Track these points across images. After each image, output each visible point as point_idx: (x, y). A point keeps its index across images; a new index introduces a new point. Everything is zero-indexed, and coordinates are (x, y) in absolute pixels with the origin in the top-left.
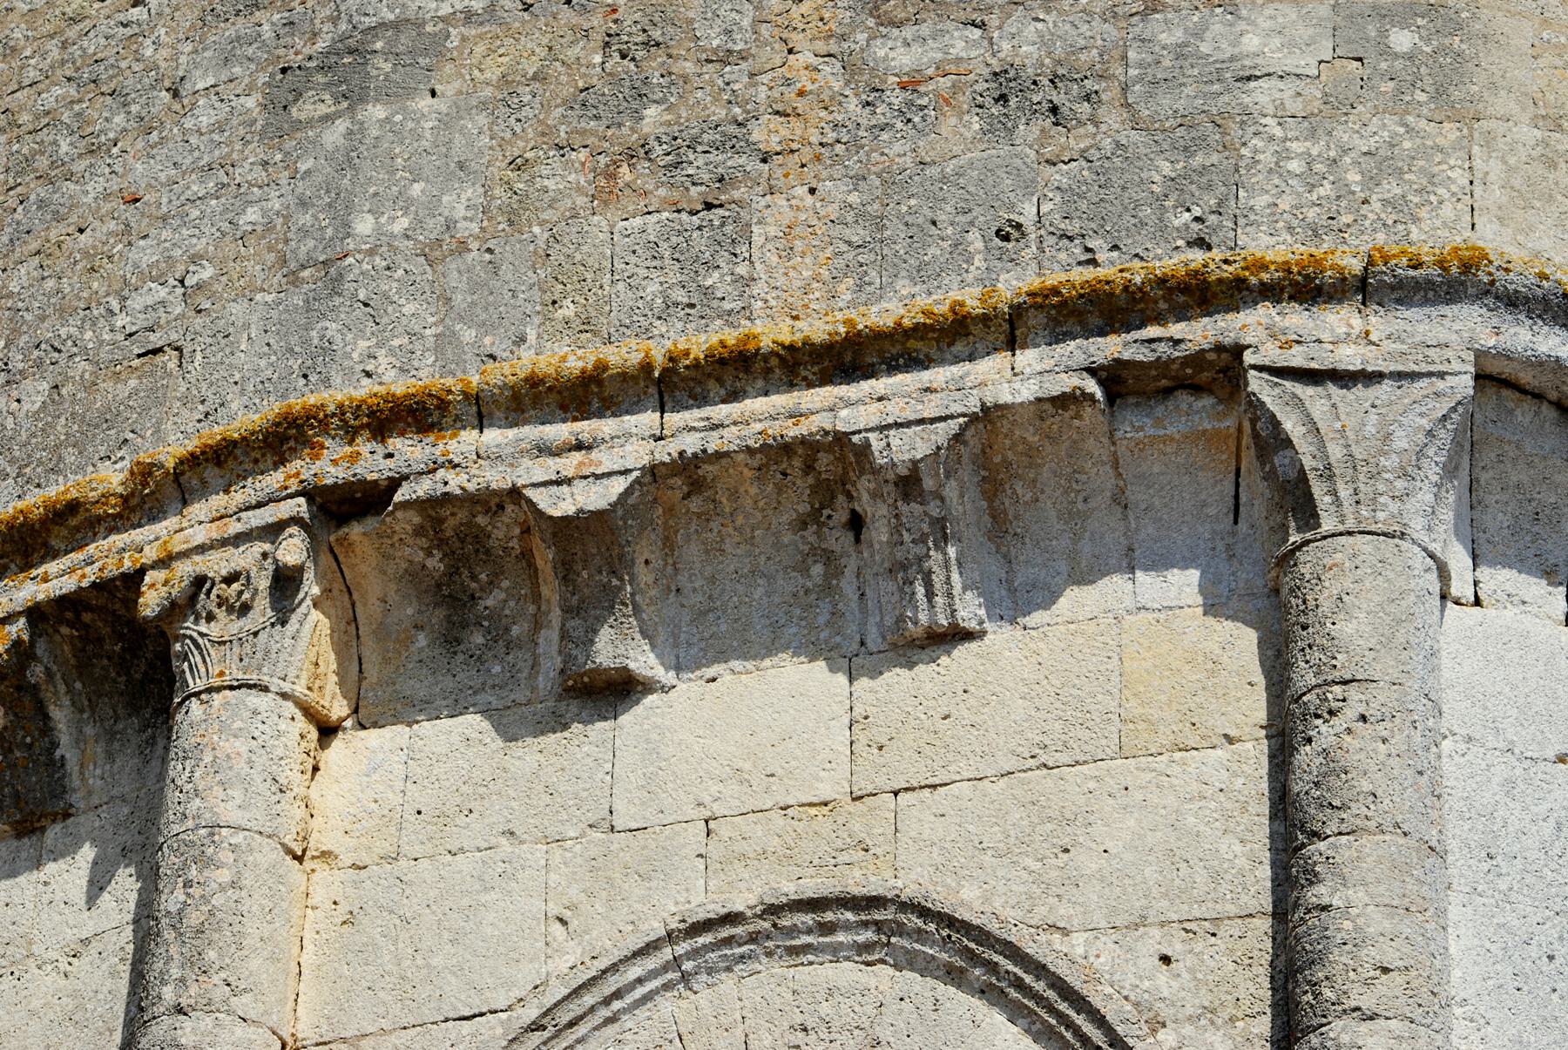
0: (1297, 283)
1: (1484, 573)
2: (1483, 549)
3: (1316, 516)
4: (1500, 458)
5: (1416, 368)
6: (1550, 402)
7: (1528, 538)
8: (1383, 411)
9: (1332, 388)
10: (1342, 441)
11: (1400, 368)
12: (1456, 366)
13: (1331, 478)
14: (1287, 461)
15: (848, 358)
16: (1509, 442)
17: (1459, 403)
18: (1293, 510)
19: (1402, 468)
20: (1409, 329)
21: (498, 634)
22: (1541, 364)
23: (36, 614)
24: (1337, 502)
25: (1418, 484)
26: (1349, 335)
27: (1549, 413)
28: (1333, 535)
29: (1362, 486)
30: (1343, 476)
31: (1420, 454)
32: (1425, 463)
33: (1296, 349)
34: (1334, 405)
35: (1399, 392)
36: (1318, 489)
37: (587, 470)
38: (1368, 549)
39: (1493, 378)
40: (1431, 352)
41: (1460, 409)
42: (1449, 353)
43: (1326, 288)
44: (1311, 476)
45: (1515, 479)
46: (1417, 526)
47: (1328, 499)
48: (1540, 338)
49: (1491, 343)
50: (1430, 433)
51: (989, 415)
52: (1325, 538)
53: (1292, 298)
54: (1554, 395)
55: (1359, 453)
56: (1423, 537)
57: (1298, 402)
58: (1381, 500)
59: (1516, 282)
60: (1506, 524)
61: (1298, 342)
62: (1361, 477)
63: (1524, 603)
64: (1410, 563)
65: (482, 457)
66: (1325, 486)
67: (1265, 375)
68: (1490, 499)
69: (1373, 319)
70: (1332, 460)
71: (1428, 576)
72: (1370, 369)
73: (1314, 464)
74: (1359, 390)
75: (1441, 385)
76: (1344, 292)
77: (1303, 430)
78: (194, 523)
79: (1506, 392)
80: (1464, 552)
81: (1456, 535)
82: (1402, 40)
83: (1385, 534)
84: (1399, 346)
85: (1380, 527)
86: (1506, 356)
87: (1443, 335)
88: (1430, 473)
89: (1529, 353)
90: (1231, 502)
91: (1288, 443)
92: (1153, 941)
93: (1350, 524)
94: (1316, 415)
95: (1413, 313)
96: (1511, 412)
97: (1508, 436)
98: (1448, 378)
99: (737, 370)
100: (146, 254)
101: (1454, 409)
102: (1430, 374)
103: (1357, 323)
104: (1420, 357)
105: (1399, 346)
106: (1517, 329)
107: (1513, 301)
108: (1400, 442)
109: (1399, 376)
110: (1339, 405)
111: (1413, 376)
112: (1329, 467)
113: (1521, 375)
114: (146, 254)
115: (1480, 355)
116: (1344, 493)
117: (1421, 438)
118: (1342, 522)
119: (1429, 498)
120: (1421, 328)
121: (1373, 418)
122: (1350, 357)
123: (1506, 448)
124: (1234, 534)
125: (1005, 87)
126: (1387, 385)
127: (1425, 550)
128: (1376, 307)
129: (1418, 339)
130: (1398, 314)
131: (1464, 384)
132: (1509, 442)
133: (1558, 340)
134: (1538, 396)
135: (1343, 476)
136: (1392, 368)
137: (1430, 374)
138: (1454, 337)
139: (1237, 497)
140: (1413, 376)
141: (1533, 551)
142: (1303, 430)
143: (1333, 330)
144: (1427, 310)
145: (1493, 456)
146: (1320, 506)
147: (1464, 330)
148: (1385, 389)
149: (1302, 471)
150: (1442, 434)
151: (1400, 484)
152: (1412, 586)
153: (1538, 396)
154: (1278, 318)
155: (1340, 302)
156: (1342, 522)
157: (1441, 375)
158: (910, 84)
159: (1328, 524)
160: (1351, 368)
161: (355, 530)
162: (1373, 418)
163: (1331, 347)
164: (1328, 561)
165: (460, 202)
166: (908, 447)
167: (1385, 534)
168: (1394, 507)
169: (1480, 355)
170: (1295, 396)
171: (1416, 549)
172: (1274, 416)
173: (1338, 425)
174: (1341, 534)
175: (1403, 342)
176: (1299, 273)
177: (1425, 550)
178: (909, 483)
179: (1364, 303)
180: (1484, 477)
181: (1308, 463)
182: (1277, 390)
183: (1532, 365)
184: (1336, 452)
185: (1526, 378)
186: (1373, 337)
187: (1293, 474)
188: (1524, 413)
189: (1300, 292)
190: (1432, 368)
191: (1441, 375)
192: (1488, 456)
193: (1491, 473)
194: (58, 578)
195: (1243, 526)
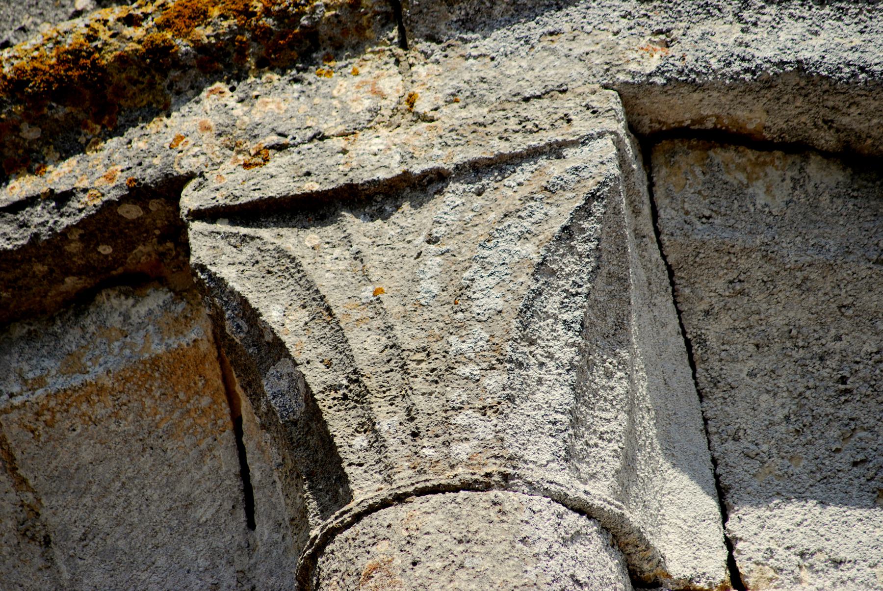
0: (267, 31)
1: (746, 521)
2: (739, 471)
3: (343, 479)
4: (738, 287)
5: (505, 148)
6: (827, 155)
7: (834, 432)
8: (451, 245)
9: (353, 224)
10: (378, 322)
11: (475, 153)
12: (582, 126)
13: (361, 398)
14: (284, 384)
16: (747, 251)
17: (593, 197)
18: (310, 476)
19: (496, 348)
20: (490, 74)
22: (768, 84)
24: (378, 443)
25: (534, 372)
26: (375, 111)
27: (823, 176)
28: (372, 509)
29: (420, 402)
30: (384, 389)
31: (527, 312)
32: (542, 328)
33: (279, 160)
34: (357, 256)
35: (478, 202)
36: (340, 424)
38: (435, 521)
40: (533, 110)
41: (598, 209)
42: (568, 104)
43: (323, 30)
44: (325, 402)
45: (779, 321)
46: (540, 457)
47: (360, 441)
48: (761, 32)
49: (652, 63)
50: (541, 268)
52: (357, 518)
53: (264, 64)
54: (827, 139)
55: (406, 336)
56: (562, 479)
57: (289, 266)
58: (460, 419)
60: (780, 414)
61: (280, 148)
62: (419, 384)
63: (837, 563)
64: (527, 530)
66: (354, 417)
67: (222, 227)
68: (737, 372)
69: (421, 71)
70: (361, 361)
71: (579, 549)
72: (417, 169)
73: (329, 378)
74: (406, 217)
75: (554, 169)
76: (360, 29)
77: (303, 315)
79: (719, 156)
80: (694, 487)
81: (670, 453)
83: (468, 486)
84: (475, 112)
85: (463, 473)
86: (686, 82)
87: (554, 70)
88: (555, 347)
89: (736, 67)
90: (234, 485)
91: (278, 349)
93: (404, 479)
94: (324, 280)
95: (495, 41)
96: (739, 192)
97: (740, 239)
98: (568, 152)
101: (584, 211)
102: (533, 154)
103: (392, 84)
104: (512, 124)
105: (475, 112)
106: (708, 25)
108: (489, 297)
109: (475, 170)
110: (366, 251)
111: (501, 165)
112: (356, 377)
113: (741, 114)
115: (632, 96)
116: (388, 420)
117: (525, 280)
118: (388, 480)
119: (562, 395)
120: (512, 67)
121: (433, 262)
122: (378, 156)
123: (743, 264)
124: (249, 548)
126: (455, 194)
127: (561, 499)
128: (424, 45)
129: (511, 86)
130: (469, 49)
131: (601, 156)
132: (747, 251)
133: (799, 28)
134: (797, 148)
135: (384, 389)
136: (458, 159)
137: (533, 154)
138: (579, 67)
139: (244, 473)
140: (501, 165)
141: (847, 456)
142: (303, 315)
143: (345, 109)
144: (521, 29)
145: (719, 284)
146: (348, 455)
148: (452, 201)
149: (310, 398)
150: (570, 264)
151: (494, 381)
152: (531, 577)
153: (797, 148)
154: (239, 110)
155: (357, 50)
156: (388, 480)
157: (555, 150)
159: (364, 488)
160: (382, 175)
162: (433, 262)
163: (341, 143)
164: (364, 563)
167: (468, 486)
168: (485, 428)
169: (632, 96)
170: (281, 253)
171: (539, 502)
172: (244, 301)
173: (367, 293)
174: (385, 504)
175: (481, 102)
176: (267, 12)
177: (561, 499)
179: (403, 45)
180: (713, 331)
181: (316, 377)
182: (249, 250)
183: (748, 89)
184: (366, 345)
185: (753, 116)
186: (423, 106)
187: (299, 409)
189: (278, 49)
190: (534, 141)
191: (555, 150)
192: (710, 288)
193: (726, 321)
195: (264, 528)
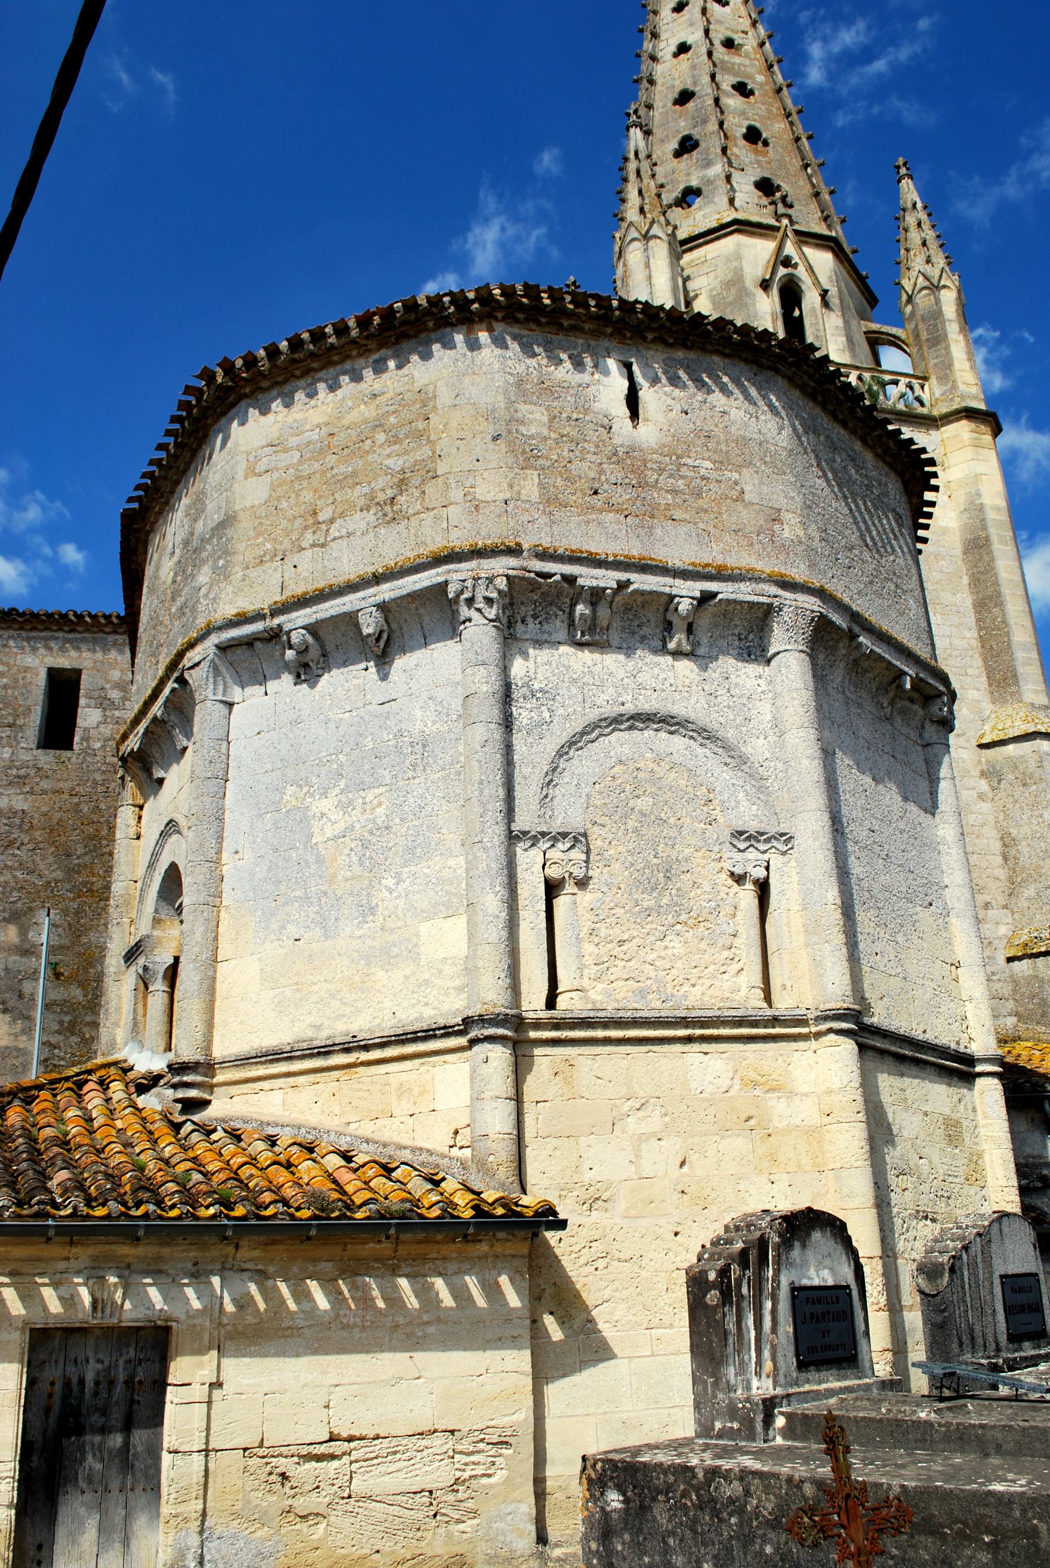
39: (223, 649)
59: (218, 624)
107: (220, 628)
122: (197, 659)
147: (214, 639)
166: (159, 714)
188: (239, 651)
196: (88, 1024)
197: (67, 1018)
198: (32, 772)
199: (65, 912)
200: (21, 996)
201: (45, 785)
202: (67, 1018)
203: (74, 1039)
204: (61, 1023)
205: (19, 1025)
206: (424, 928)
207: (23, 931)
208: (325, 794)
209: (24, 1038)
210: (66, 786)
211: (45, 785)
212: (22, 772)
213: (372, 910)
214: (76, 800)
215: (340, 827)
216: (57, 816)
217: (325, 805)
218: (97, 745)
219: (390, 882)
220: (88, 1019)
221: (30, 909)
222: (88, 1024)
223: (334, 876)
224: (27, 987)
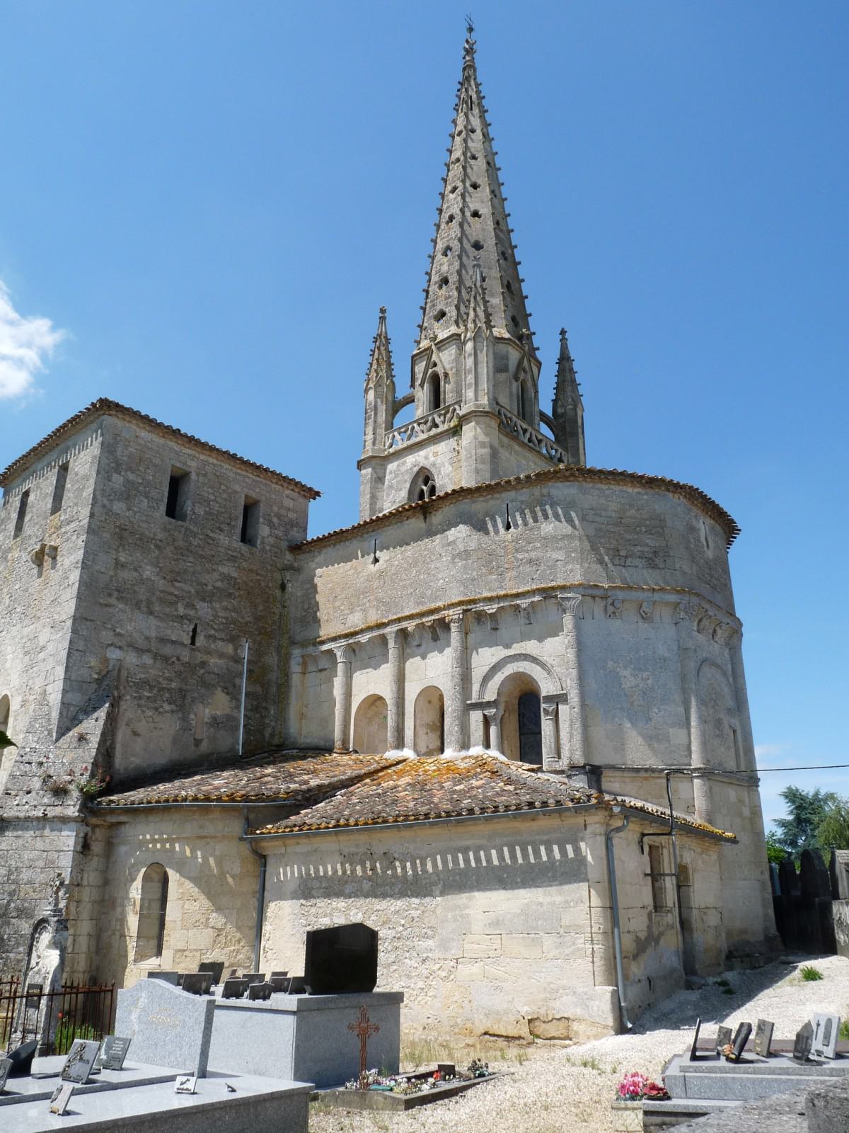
15: (517, 596)
21: (484, 623)
23: (434, 620)
37: (492, 609)
51: (532, 602)
65: (480, 607)
78: (451, 612)
82: (573, 555)
92: (553, 658)
99: (506, 597)
100: (440, 576)
114: (440, 576)
125: (530, 561)
158: (522, 560)
161: (468, 613)
165: (475, 573)
166: (524, 606)
178: (525, 609)
194: (436, 617)
196: (263, 708)
197: (255, 703)
198: (239, 555)
199: (254, 642)
200: (234, 686)
201: (245, 564)
202: (255, 703)
203: (258, 715)
204: (252, 705)
205: (234, 703)
206: (671, 730)
207: (236, 649)
208: (625, 668)
209: (236, 711)
210: (254, 568)
211: (245, 564)
212: (235, 554)
213: (650, 719)
214: (258, 578)
215: (633, 684)
216: (251, 584)
217: (626, 673)
218: (268, 548)
219: (657, 711)
220: (264, 705)
221: (238, 636)
222: (263, 708)
223: (632, 702)
224: (237, 681)
